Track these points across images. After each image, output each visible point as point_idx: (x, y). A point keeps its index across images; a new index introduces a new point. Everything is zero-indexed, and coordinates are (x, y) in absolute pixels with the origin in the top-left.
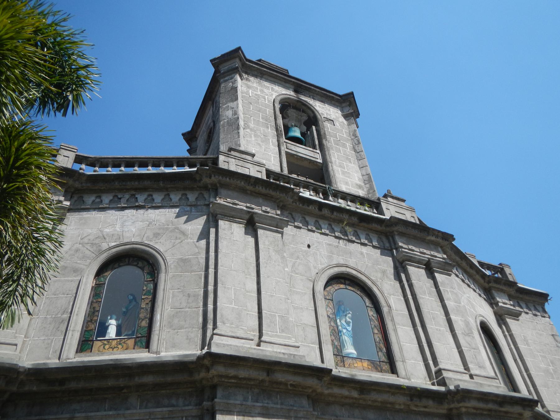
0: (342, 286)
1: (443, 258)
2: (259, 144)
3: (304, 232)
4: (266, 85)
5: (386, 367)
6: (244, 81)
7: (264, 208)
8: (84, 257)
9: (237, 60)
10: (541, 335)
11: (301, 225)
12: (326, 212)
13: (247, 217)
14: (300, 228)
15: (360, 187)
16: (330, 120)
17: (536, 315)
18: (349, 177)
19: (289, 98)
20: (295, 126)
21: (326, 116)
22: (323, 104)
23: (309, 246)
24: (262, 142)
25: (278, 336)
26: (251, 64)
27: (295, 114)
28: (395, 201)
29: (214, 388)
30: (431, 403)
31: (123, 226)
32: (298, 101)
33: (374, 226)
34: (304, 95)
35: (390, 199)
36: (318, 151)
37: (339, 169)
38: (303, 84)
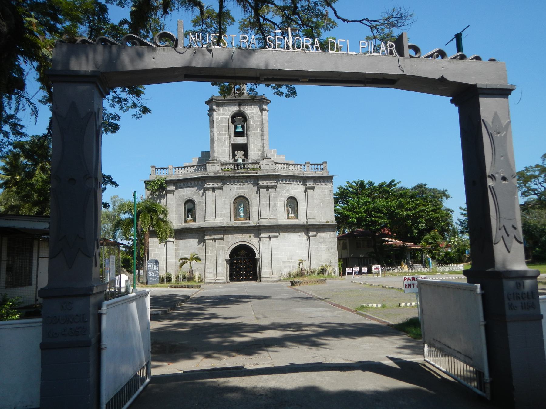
2: (222, 146)
3: (230, 185)
5: (248, 218)
6: (218, 112)
7: (217, 183)
8: (181, 201)
9: (213, 103)
10: (324, 191)
12: (236, 178)
15: (260, 150)
17: (326, 184)
18: (256, 147)
21: (251, 115)
22: (251, 106)
24: (223, 144)
28: (267, 160)
29: (205, 231)
31: (187, 192)
34: (243, 106)
35: (264, 160)
36: (246, 137)
37: (253, 144)
38: (242, 101)
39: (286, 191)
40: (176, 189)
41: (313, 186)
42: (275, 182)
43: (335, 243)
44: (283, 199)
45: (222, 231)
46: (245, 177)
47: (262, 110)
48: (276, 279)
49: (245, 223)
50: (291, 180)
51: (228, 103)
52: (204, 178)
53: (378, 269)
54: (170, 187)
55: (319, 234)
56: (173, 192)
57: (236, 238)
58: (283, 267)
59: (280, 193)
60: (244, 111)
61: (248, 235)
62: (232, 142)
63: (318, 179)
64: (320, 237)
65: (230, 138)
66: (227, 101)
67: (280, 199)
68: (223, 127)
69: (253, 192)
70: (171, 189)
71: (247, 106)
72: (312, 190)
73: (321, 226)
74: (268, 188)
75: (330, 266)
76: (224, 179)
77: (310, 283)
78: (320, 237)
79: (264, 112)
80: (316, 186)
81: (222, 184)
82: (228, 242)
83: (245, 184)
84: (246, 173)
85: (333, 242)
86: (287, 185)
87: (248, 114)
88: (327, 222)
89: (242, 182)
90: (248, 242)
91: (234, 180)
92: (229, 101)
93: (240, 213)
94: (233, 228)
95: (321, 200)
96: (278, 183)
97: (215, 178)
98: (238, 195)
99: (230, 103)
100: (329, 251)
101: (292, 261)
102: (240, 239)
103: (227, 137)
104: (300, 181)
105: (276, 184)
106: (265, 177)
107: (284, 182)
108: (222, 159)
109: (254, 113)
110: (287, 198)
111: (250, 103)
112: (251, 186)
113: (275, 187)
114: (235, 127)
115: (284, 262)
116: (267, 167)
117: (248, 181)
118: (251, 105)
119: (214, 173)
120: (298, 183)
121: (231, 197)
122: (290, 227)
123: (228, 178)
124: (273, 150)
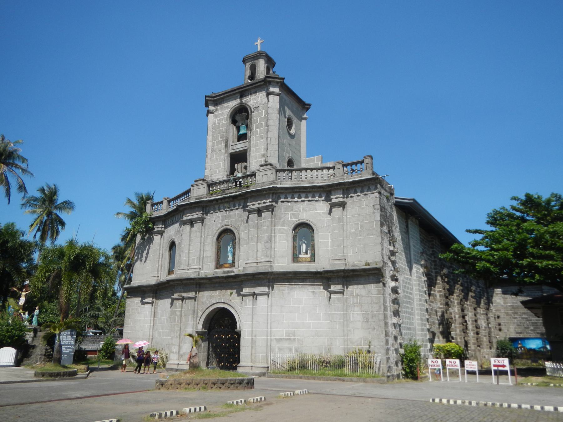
0: (226, 234)
1: (270, 202)
4: (225, 106)
7: (196, 213)
11: (212, 212)
12: (219, 201)
13: (190, 221)
14: (212, 213)
16: (257, 107)
17: (366, 195)
19: (235, 108)
20: (242, 125)
21: (255, 106)
23: (214, 221)
24: (218, 156)
25: (195, 265)
26: (216, 98)
27: (239, 118)
30: (232, 279)
32: (240, 106)
33: (240, 198)
34: (246, 96)
38: (242, 89)
39: (293, 214)
40: (165, 228)
41: (341, 200)
42: (271, 200)
43: (380, 306)
44: (286, 228)
45: (194, 286)
46: (231, 199)
47: (269, 94)
48: (258, 371)
49: (228, 272)
50: (303, 195)
51: (228, 98)
52: (184, 207)
53: (504, 366)
54: (158, 226)
55: (351, 287)
56: (161, 233)
57: (213, 297)
58: (277, 350)
59: (280, 218)
60: (246, 103)
61: (229, 291)
62: (231, 152)
63: (352, 188)
64: (352, 294)
65: (226, 146)
66: (224, 95)
67: (280, 229)
68: (219, 133)
69: (242, 221)
70: (160, 229)
71: (251, 94)
72: (339, 208)
73: (351, 273)
74: (259, 212)
75: (369, 352)
76: (207, 206)
77: (187, 386)
78: (352, 294)
79: (271, 97)
80: (348, 201)
81: (203, 214)
82: (203, 304)
83: (232, 210)
84: (236, 192)
85: (376, 303)
86: (293, 204)
87: (251, 106)
88: (366, 265)
89: (229, 208)
90: (228, 304)
91: (219, 206)
92: (227, 94)
93: (228, 257)
94: (208, 281)
95: (358, 224)
96: (277, 202)
97: (193, 206)
98: (222, 229)
99: (230, 97)
100: (367, 321)
101: (294, 340)
102: (217, 298)
103: (223, 145)
104: (320, 194)
105: (274, 204)
106: (256, 194)
107: (289, 199)
108: (215, 178)
109: (259, 103)
110: (293, 226)
111: (254, 90)
112: (240, 211)
113: (271, 209)
114: (238, 129)
115: (279, 340)
116: (265, 179)
117: (237, 205)
118: (256, 92)
119: (196, 199)
120: (317, 198)
121: (215, 232)
122: (290, 275)
123: (209, 204)
124: (315, 157)
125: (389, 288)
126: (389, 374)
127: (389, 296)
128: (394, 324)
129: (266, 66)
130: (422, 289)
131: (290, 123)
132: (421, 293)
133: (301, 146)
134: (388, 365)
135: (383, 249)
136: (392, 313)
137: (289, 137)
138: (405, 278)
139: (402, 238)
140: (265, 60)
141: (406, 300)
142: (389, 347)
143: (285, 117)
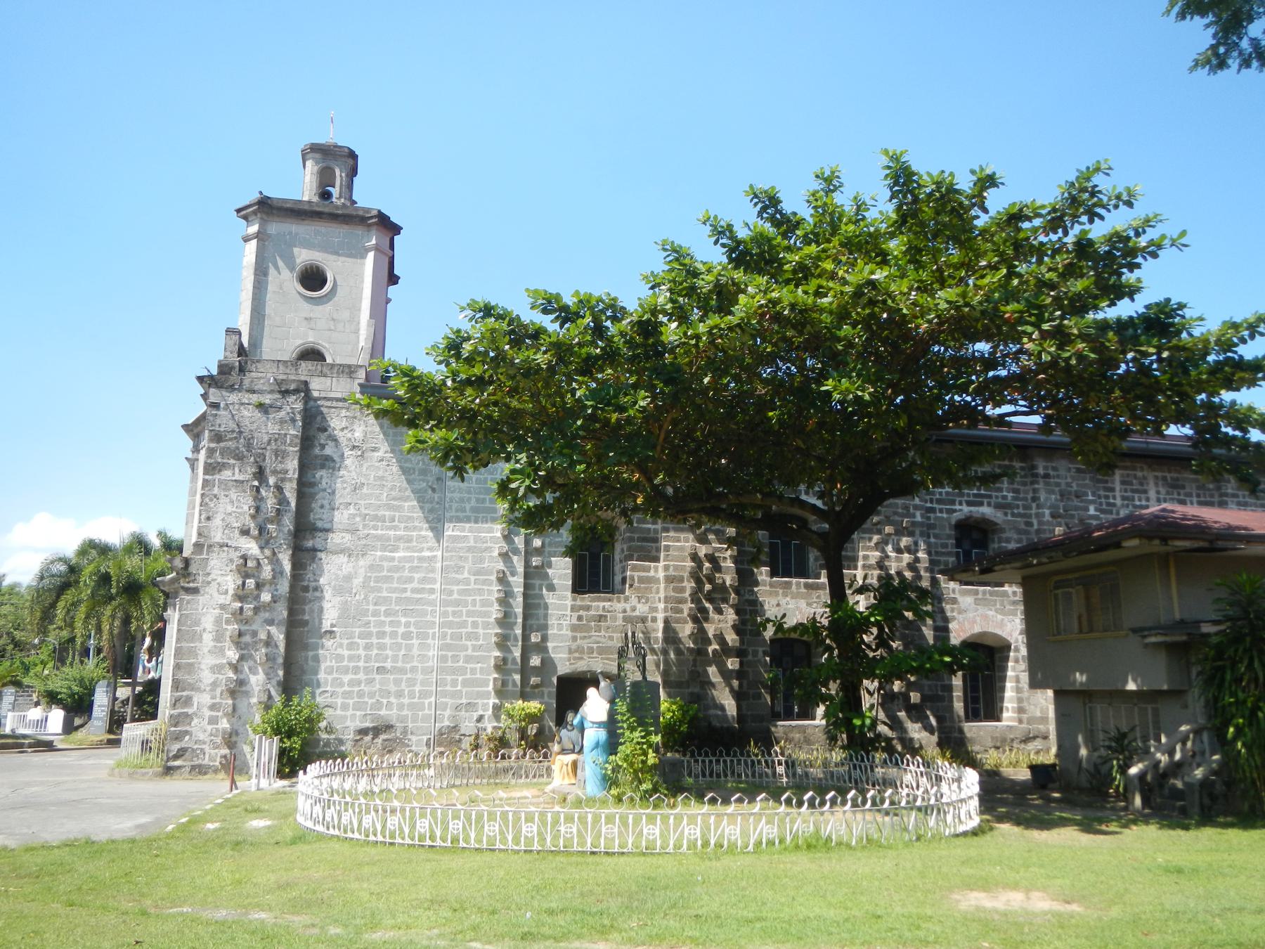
125: (226, 592)
126: (177, 763)
127: (217, 611)
128: (235, 668)
129: (316, 168)
130: (473, 578)
131: (313, 279)
132: (455, 588)
133: (360, 310)
134: (175, 747)
135: (208, 518)
136: (228, 643)
137: (306, 306)
138: (393, 559)
139: (405, 471)
140: (313, 159)
141: (383, 609)
142: (190, 711)
143: (292, 269)
